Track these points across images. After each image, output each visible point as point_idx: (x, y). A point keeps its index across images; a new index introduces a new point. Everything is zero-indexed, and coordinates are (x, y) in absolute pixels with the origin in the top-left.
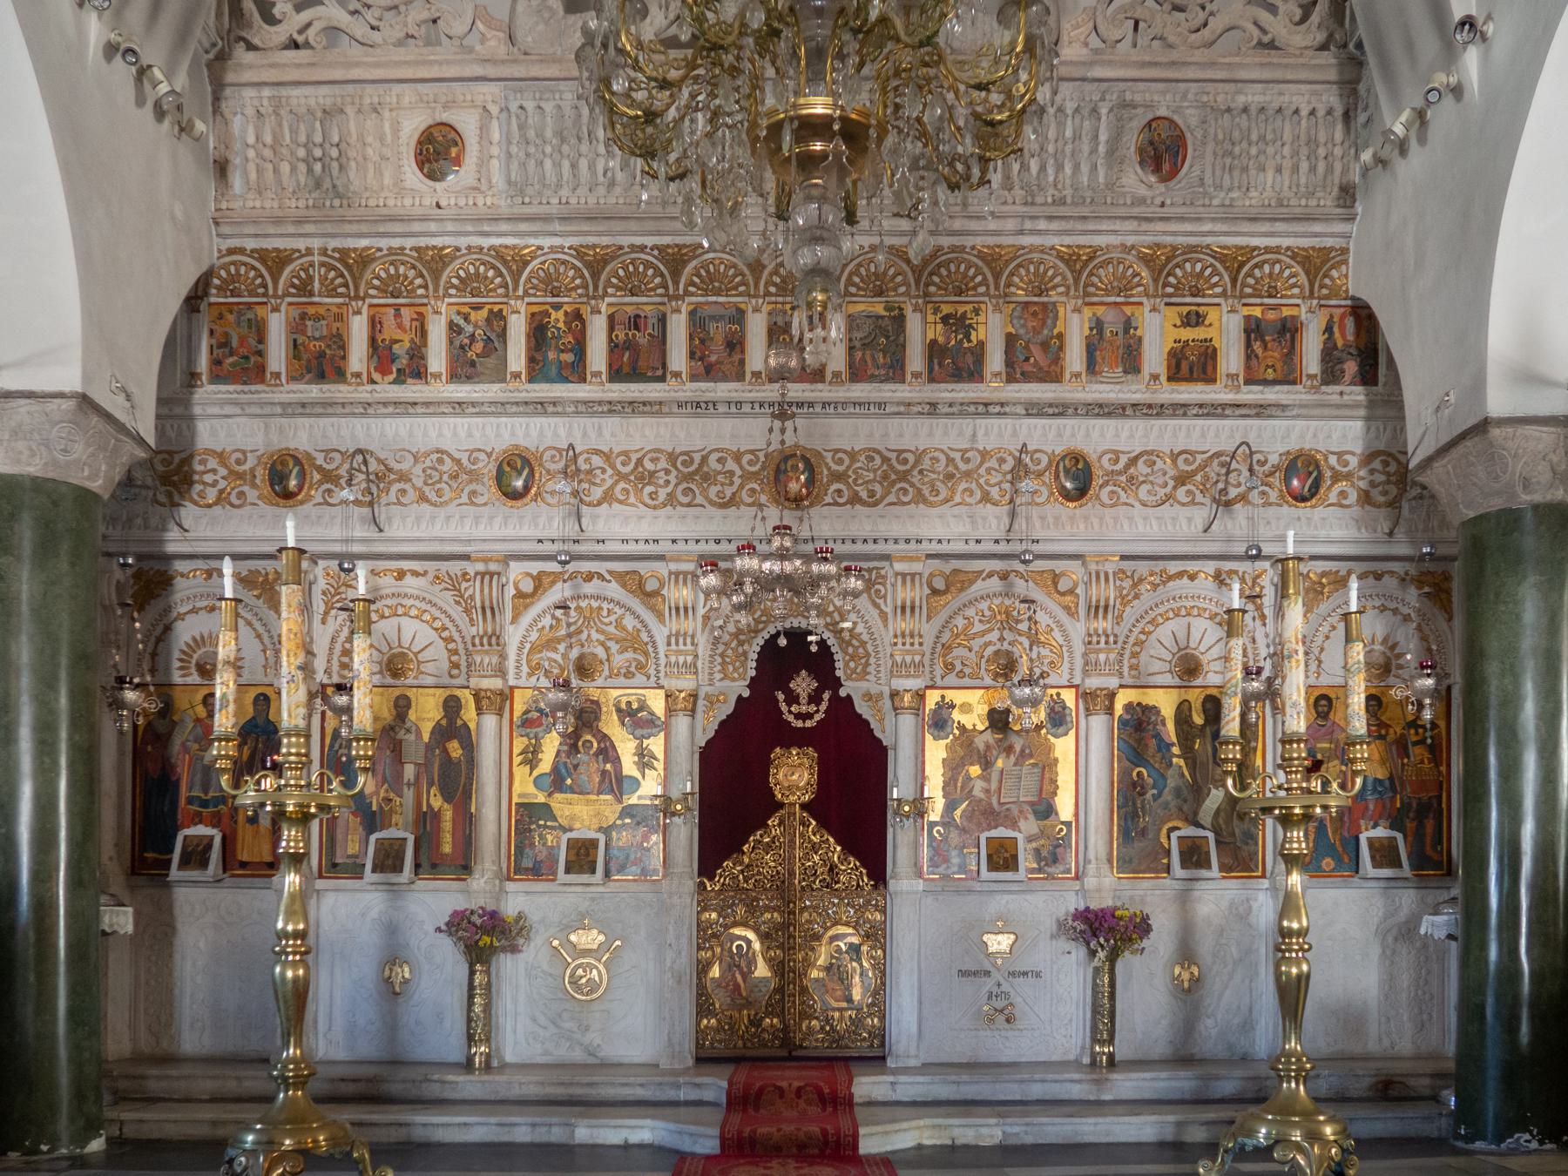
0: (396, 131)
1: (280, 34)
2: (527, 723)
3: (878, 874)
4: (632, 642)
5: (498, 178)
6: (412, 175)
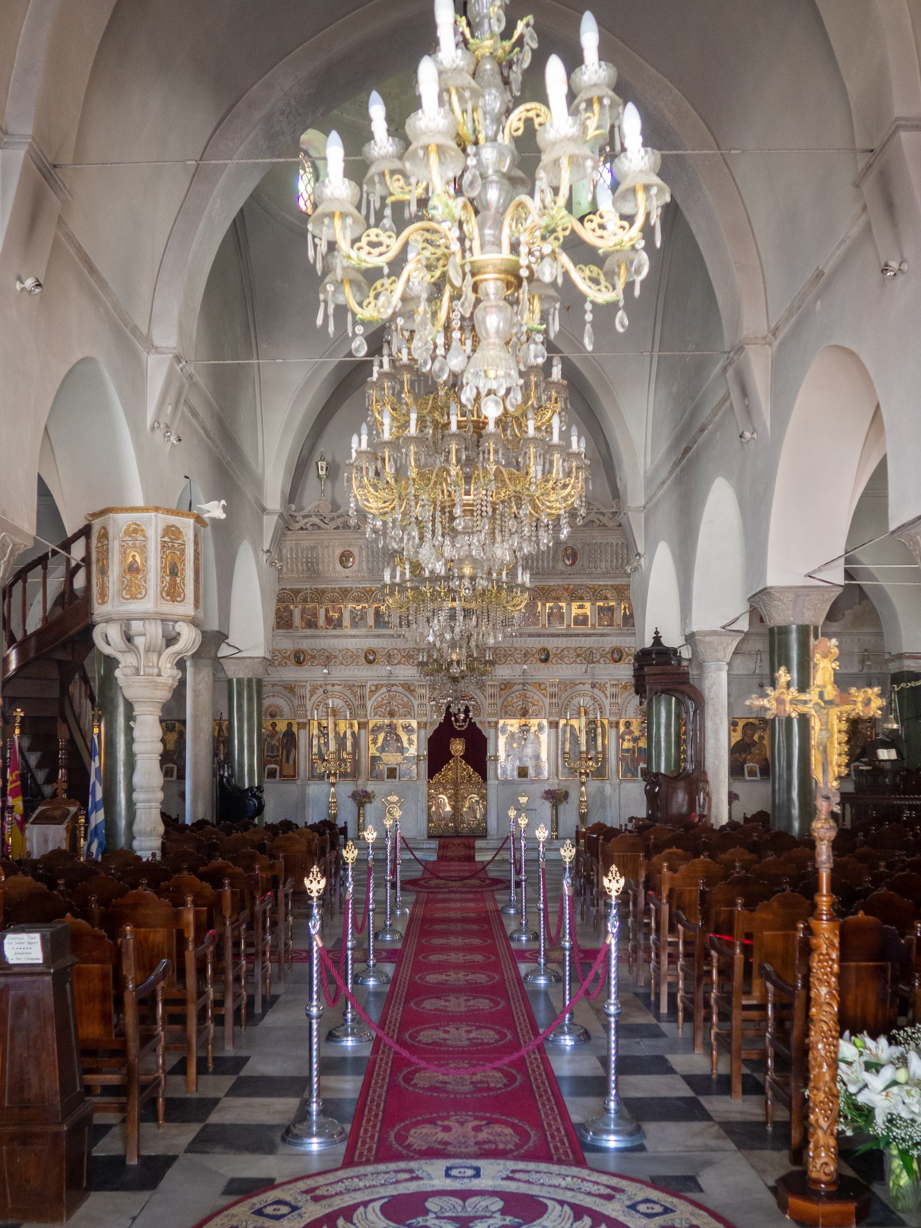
0: (333, 553)
1: (298, 526)
2: (373, 731)
3: (485, 778)
4: (404, 705)
5: (365, 567)
6: (339, 567)
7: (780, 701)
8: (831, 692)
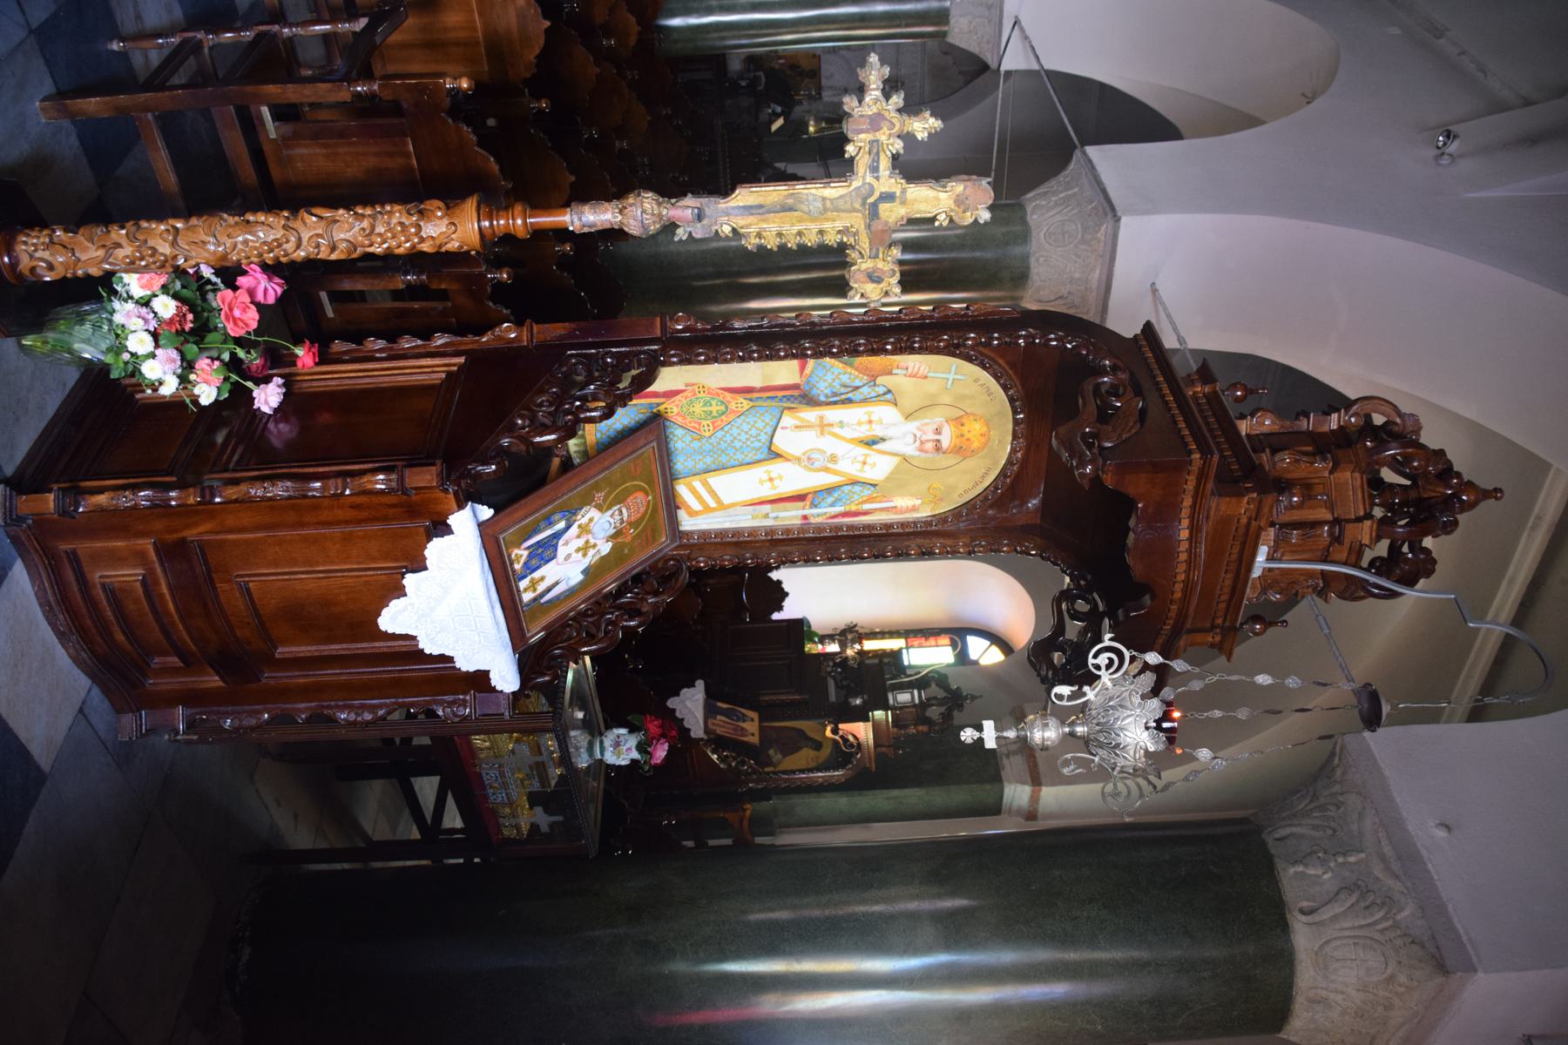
7: (876, 122)
8: (892, 213)
